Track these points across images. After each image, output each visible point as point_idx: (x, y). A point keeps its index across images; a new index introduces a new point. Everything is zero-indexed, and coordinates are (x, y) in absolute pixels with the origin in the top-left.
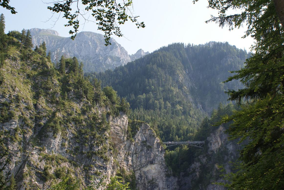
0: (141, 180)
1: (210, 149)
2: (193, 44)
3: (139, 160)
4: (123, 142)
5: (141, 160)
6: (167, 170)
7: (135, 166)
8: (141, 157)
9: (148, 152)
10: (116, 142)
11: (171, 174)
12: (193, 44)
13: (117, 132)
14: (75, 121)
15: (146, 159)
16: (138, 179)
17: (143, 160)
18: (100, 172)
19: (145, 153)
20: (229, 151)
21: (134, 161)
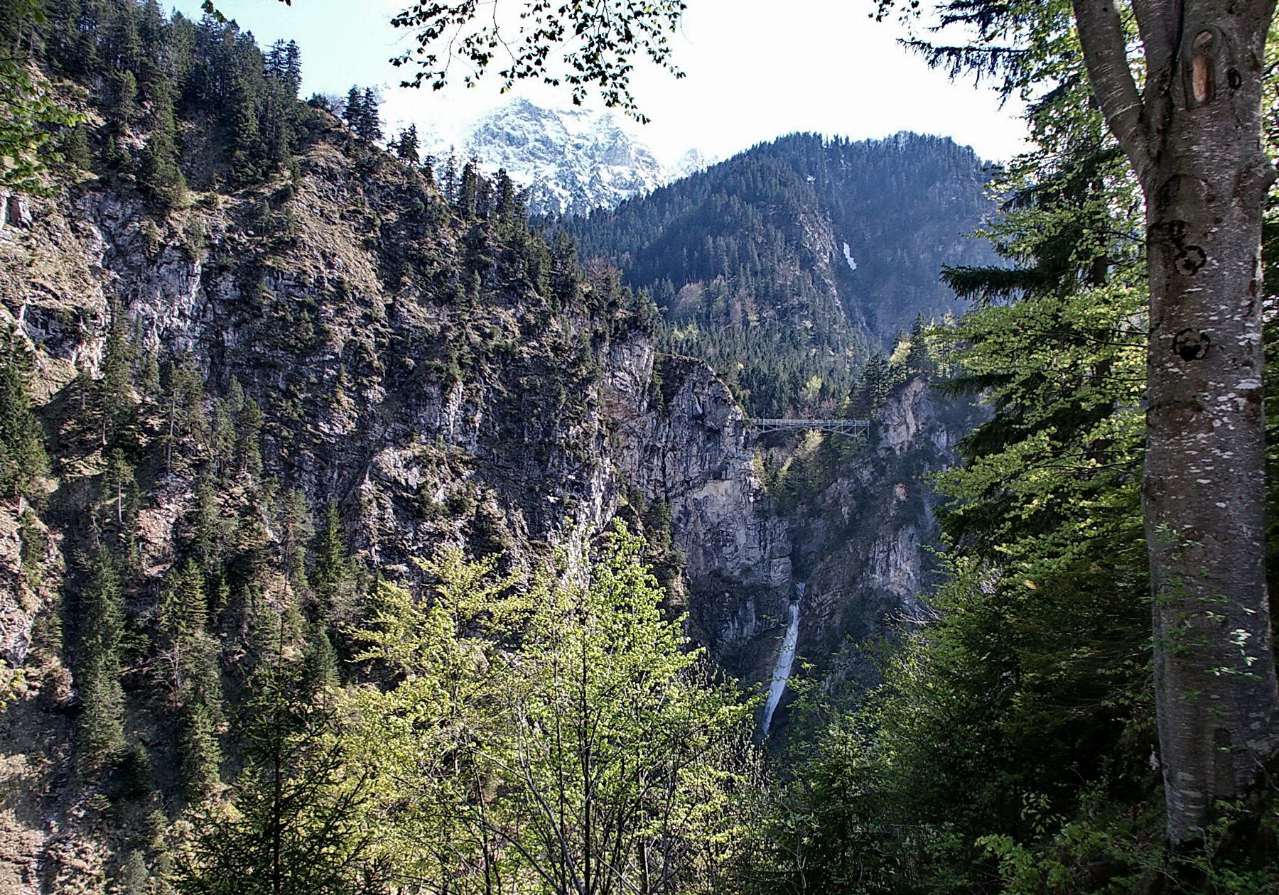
0: (686, 525)
1: (883, 444)
2: (847, 139)
3: (682, 470)
4: (639, 416)
5: (686, 469)
6: (759, 498)
7: (669, 485)
8: (689, 456)
9: (709, 445)
10: (618, 417)
11: (769, 509)
12: (847, 139)
13: (622, 387)
14: (504, 354)
15: (702, 466)
16: (679, 519)
17: (694, 470)
18: (572, 497)
19: (699, 448)
20: (939, 451)
21: (667, 471)
